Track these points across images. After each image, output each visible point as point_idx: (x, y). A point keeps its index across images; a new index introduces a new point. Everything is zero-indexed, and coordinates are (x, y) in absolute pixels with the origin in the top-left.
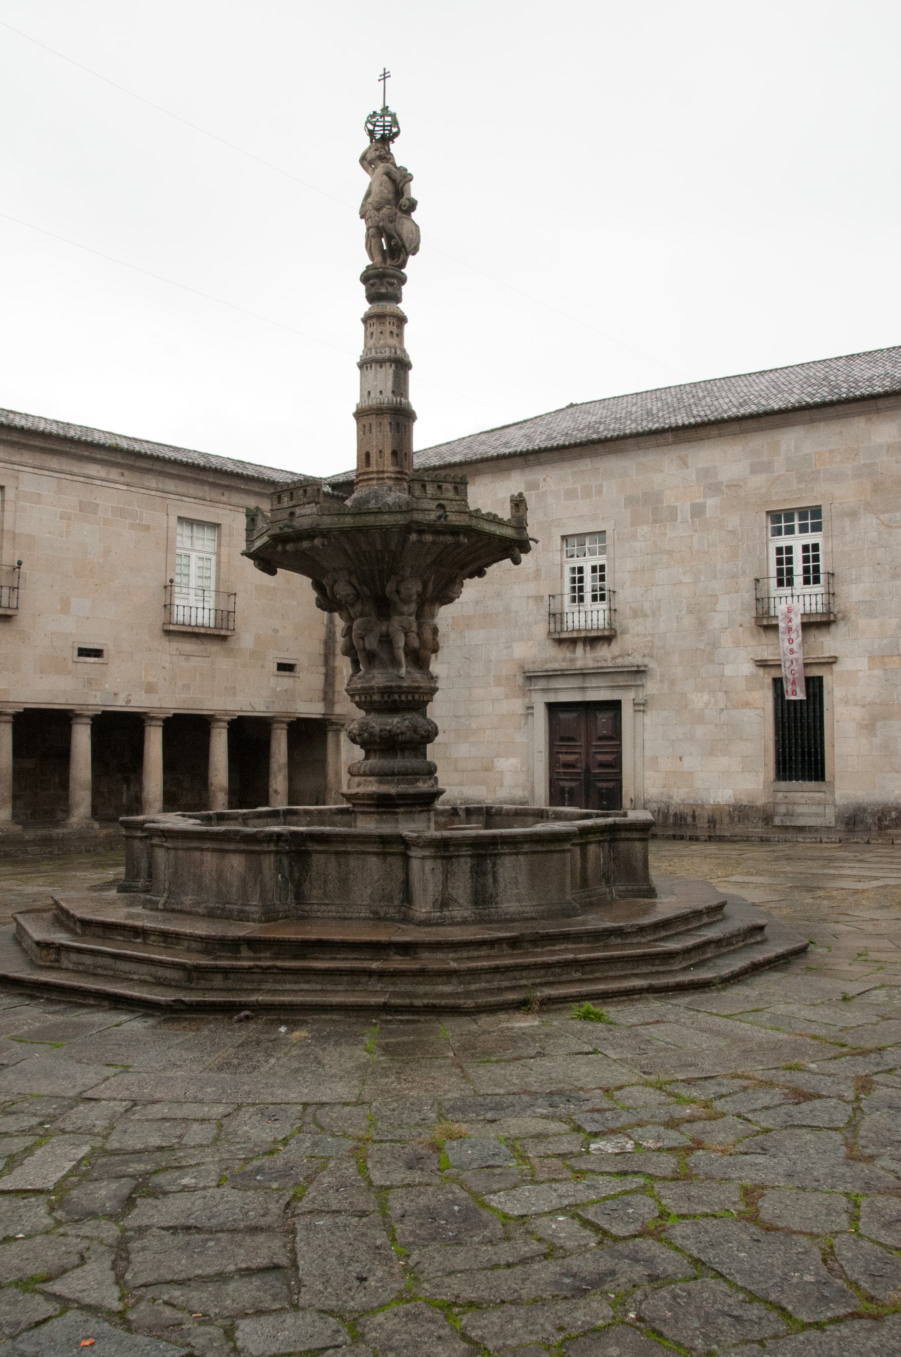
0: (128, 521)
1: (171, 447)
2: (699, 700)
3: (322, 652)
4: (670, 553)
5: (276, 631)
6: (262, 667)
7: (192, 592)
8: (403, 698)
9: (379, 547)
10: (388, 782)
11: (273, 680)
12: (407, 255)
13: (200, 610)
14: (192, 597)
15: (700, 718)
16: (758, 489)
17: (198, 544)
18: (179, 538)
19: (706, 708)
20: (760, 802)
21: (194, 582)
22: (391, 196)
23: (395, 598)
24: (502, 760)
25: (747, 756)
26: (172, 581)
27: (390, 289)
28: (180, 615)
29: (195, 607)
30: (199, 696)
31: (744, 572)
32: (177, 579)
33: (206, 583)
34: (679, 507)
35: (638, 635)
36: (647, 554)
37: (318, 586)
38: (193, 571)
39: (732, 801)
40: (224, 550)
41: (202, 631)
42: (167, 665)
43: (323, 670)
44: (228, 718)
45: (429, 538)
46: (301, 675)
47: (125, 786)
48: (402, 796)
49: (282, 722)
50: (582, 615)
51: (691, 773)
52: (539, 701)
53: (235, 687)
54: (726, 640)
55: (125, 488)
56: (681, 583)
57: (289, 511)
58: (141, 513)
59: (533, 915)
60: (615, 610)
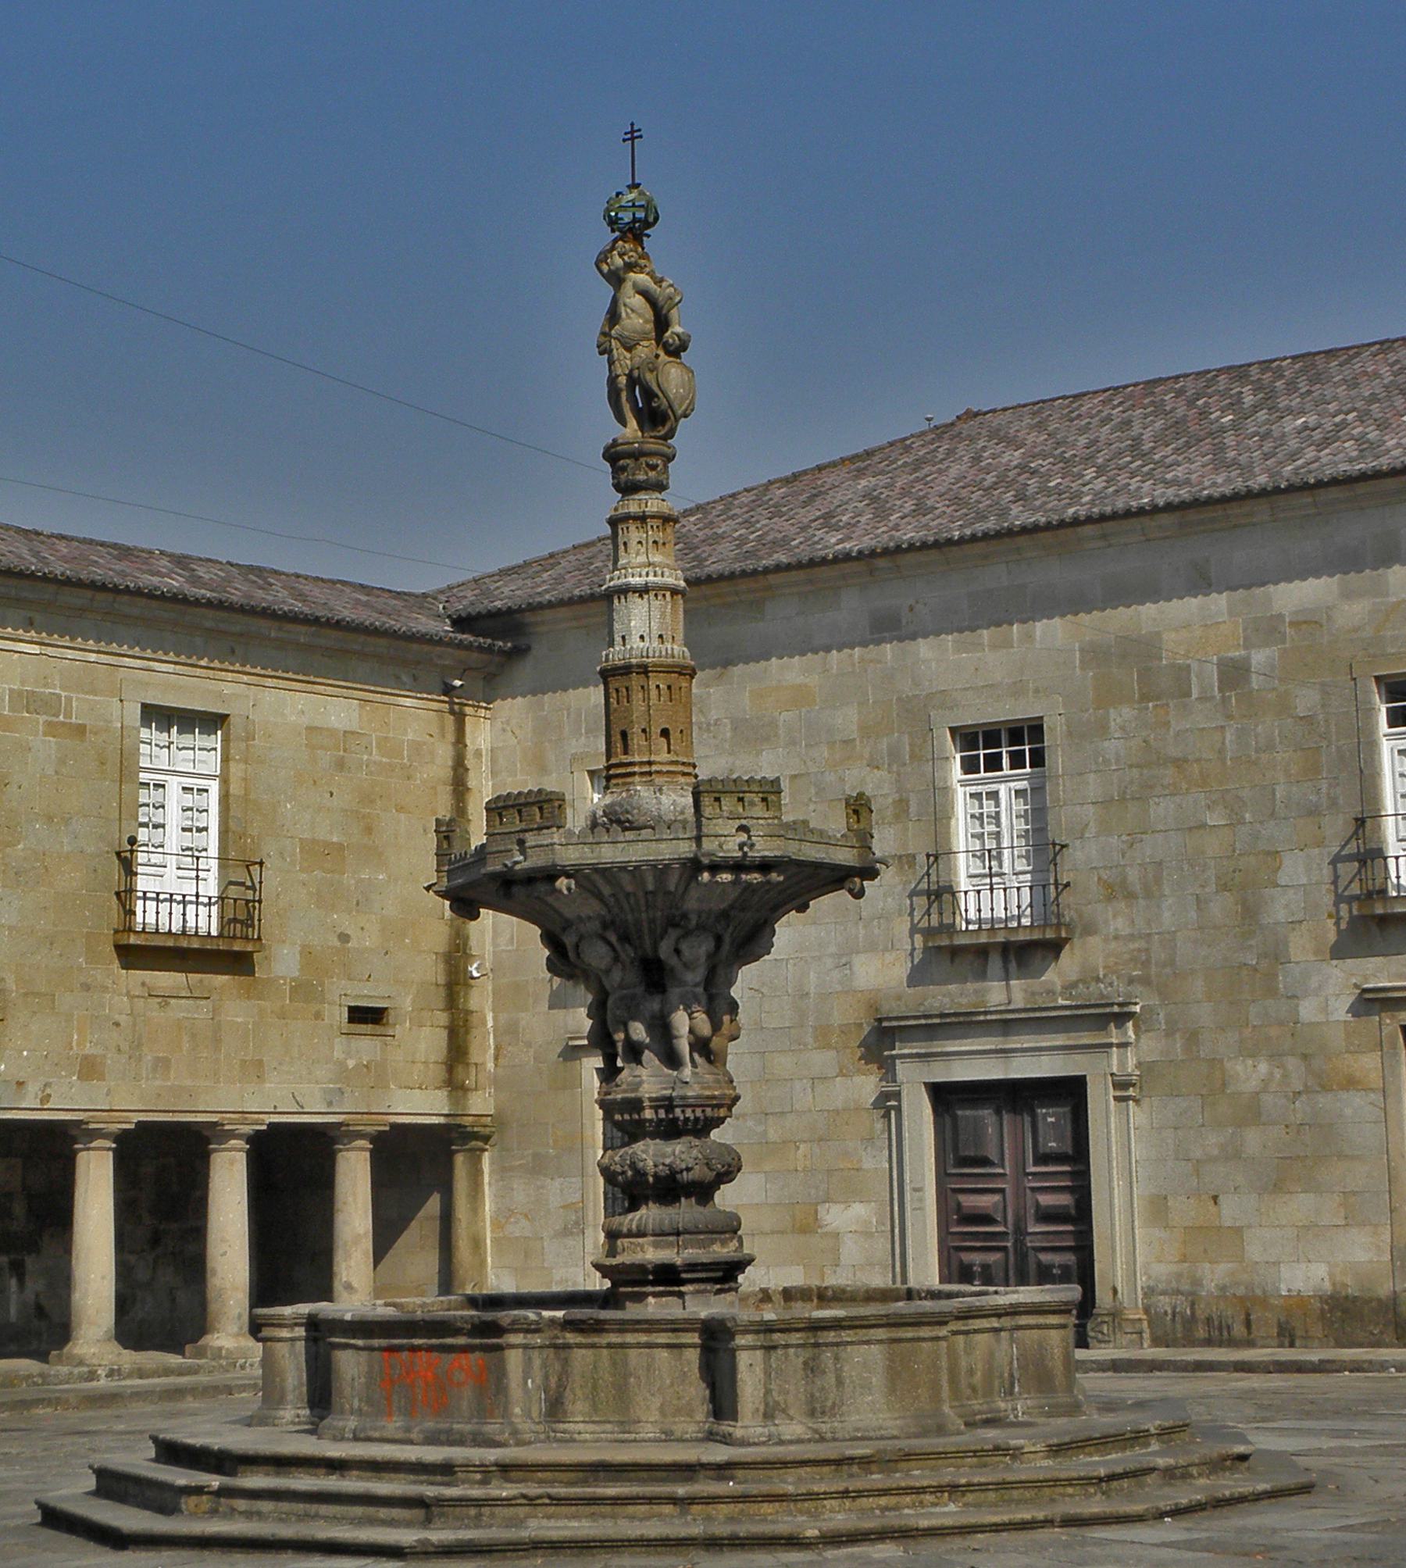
0: (42, 719)
1: (115, 546)
2: (1250, 1074)
3: (442, 980)
4: (1179, 763)
5: (344, 938)
6: (318, 1016)
7: (172, 862)
8: (689, 1113)
9: (650, 887)
10: (670, 1245)
11: (339, 1046)
12: (677, 420)
14: (171, 872)
15: (1251, 1112)
16: (1356, 630)
17: (183, 761)
18: (144, 749)
19: (1265, 1090)
20: (1384, 1290)
21: (174, 839)
22: (650, 326)
23: (673, 961)
24: (835, 1209)
25: (1354, 1193)
26: (133, 841)
27: (652, 474)
28: (146, 915)
29: (179, 889)
30: (188, 1082)
31: (1333, 803)
32: (143, 835)
33: (199, 840)
34: (1195, 666)
35: (1116, 938)
36: (1131, 766)
37: (551, 939)
38: (173, 817)
39: (1327, 1286)
40: (235, 769)
42: (123, 1019)
43: (443, 1018)
44: (247, 1129)
45: (726, 877)
46: (398, 1030)
47: (13, 1282)
48: (692, 1267)
49: (360, 1135)
50: (999, 894)
51: (1238, 1231)
52: (913, 1082)
53: (260, 1062)
54: (1300, 947)
55: (36, 649)
56: (1203, 826)
58: (69, 700)
59: (895, 1433)
60: (1067, 885)
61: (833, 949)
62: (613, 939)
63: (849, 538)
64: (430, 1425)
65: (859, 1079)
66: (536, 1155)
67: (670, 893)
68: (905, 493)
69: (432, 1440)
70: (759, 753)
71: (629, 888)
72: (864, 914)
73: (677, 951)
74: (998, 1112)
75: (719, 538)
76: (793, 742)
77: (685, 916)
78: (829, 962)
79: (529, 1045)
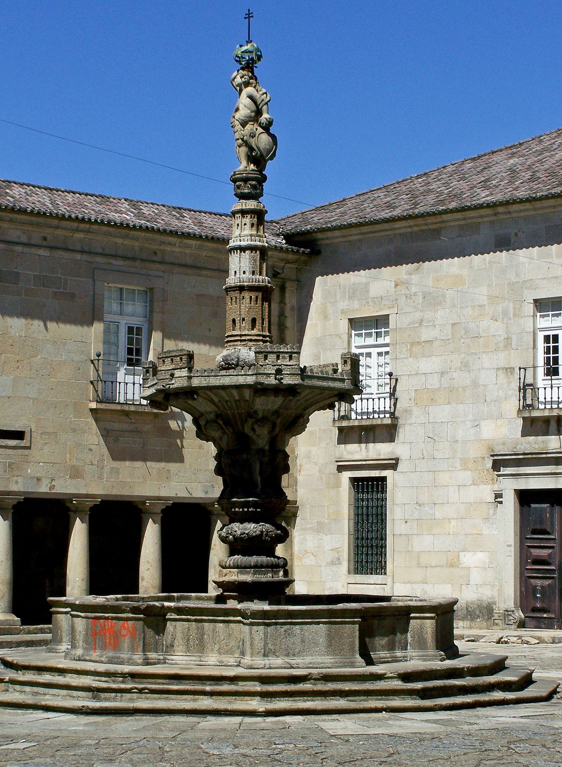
9: (237, 398)
13: (130, 386)
23: (251, 434)
24: (469, 555)
30: (129, 480)
41: (132, 408)
52: (509, 487)
57: (170, 373)
61: (471, 417)
62: (221, 422)
63: (492, 194)
64: (111, 654)
65: (482, 487)
66: (318, 523)
67: (247, 401)
68: (529, 168)
69: (110, 662)
70: (436, 311)
71: (227, 398)
72: (487, 399)
73: (253, 430)
74: (552, 505)
75: (430, 191)
76: (454, 306)
77: (256, 412)
78: (469, 424)
79: (316, 464)
